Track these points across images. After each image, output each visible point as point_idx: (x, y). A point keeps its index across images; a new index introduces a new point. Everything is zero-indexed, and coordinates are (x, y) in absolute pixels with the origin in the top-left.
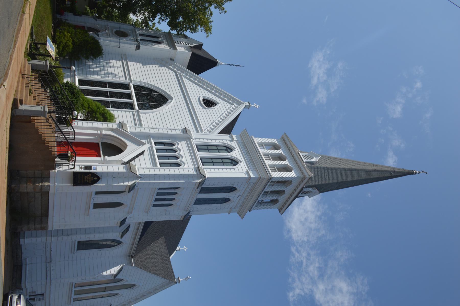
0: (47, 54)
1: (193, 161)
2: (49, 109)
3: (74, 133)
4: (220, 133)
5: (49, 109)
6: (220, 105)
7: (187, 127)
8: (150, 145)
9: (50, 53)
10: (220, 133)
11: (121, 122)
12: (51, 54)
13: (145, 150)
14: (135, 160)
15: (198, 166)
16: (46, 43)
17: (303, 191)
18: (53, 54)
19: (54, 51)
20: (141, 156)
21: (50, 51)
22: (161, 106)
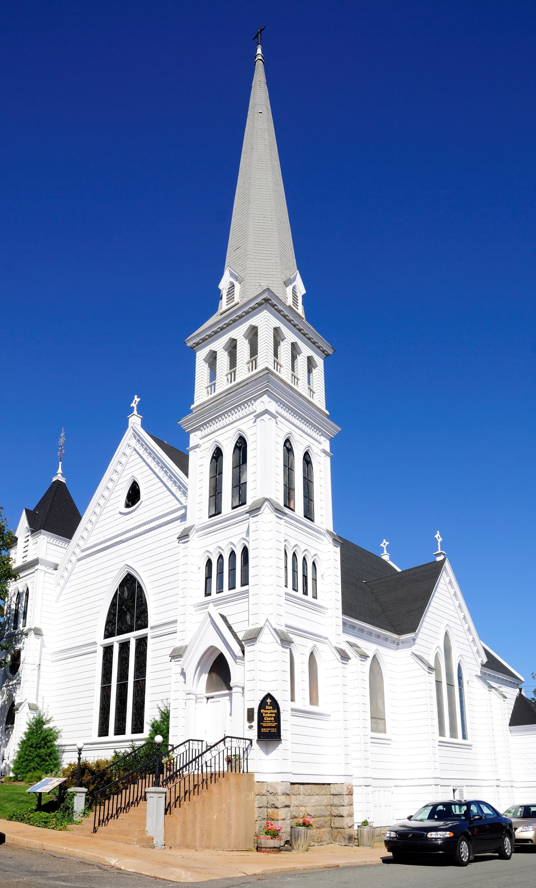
0: (58, 791)
1: (238, 523)
2: (151, 784)
3: (191, 742)
4: (187, 474)
5: (151, 784)
6: (135, 474)
7: (177, 536)
8: (209, 603)
9: (56, 786)
10: (187, 474)
11: (171, 658)
12: (58, 783)
13: (219, 614)
14: (235, 632)
15: (246, 513)
16: (38, 792)
17: (293, 305)
18: (57, 781)
19: (51, 780)
20: (228, 621)
21: (52, 786)
22: (140, 587)
